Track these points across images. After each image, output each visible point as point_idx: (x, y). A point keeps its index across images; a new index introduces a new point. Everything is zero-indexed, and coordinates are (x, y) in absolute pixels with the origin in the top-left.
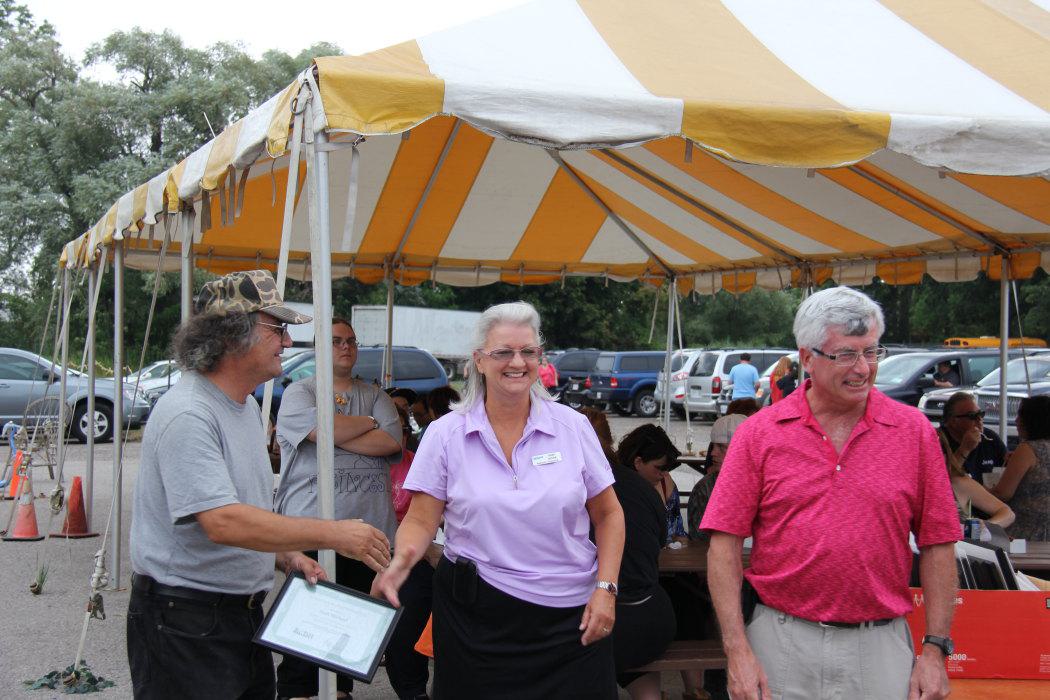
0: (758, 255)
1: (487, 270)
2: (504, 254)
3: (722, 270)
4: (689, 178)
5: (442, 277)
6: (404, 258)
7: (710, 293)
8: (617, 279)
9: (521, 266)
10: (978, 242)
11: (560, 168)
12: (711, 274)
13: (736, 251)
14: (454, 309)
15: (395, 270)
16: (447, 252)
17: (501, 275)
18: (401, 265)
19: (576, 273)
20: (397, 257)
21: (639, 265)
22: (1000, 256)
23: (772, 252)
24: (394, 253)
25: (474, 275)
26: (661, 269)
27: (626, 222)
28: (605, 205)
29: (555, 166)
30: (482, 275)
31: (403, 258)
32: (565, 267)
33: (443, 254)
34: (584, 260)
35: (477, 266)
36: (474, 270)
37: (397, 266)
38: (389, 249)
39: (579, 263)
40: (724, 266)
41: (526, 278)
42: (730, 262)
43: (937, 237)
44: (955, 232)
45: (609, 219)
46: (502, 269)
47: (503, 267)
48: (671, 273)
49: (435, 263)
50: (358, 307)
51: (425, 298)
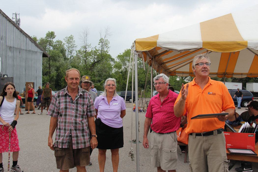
1: (243, 75)
2: (247, 72)
5: (234, 76)
6: (227, 74)
9: (251, 74)
15: (226, 75)
16: (235, 72)
17: (247, 76)
18: (226, 75)
20: (225, 73)
24: (225, 72)
25: (241, 76)
29: (254, 55)
30: (243, 76)
31: (227, 73)
33: (234, 72)
35: (242, 74)
37: (226, 75)
38: (224, 71)
41: (252, 76)
47: (247, 74)
49: (233, 74)
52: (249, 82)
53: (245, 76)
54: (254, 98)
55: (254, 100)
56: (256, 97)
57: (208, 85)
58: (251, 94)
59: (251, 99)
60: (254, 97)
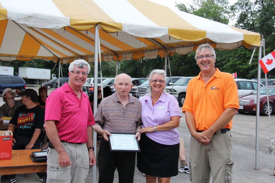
0: (74, 55)
3: (68, 58)
4: (52, 37)
7: (65, 63)
8: (46, 60)
9: (22, 56)
10: (111, 52)
11: (26, 34)
12: (66, 59)
13: (70, 54)
14: (44, 68)
17: (17, 58)
19: (36, 58)
21: (52, 57)
22: (116, 56)
23: (75, 54)
25: (9, 58)
26: (57, 58)
27: (47, 48)
28: (41, 43)
29: (25, 33)
30: (11, 58)
32: (33, 57)
34: (37, 55)
35: (10, 56)
36: (9, 57)
39: (36, 56)
40: (68, 57)
42: (69, 56)
43: (104, 51)
44: (107, 50)
45: (41, 46)
46: (17, 57)
47: (17, 56)
48: (59, 59)
50: (20, 68)
51: (37, 66)
52: (22, 67)
53: (15, 59)
54: (27, 85)
55: (27, 88)
56: (30, 84)
57: (212, 78)
58: (22, 80)
59: (23, 87)
60: (27, 84)
